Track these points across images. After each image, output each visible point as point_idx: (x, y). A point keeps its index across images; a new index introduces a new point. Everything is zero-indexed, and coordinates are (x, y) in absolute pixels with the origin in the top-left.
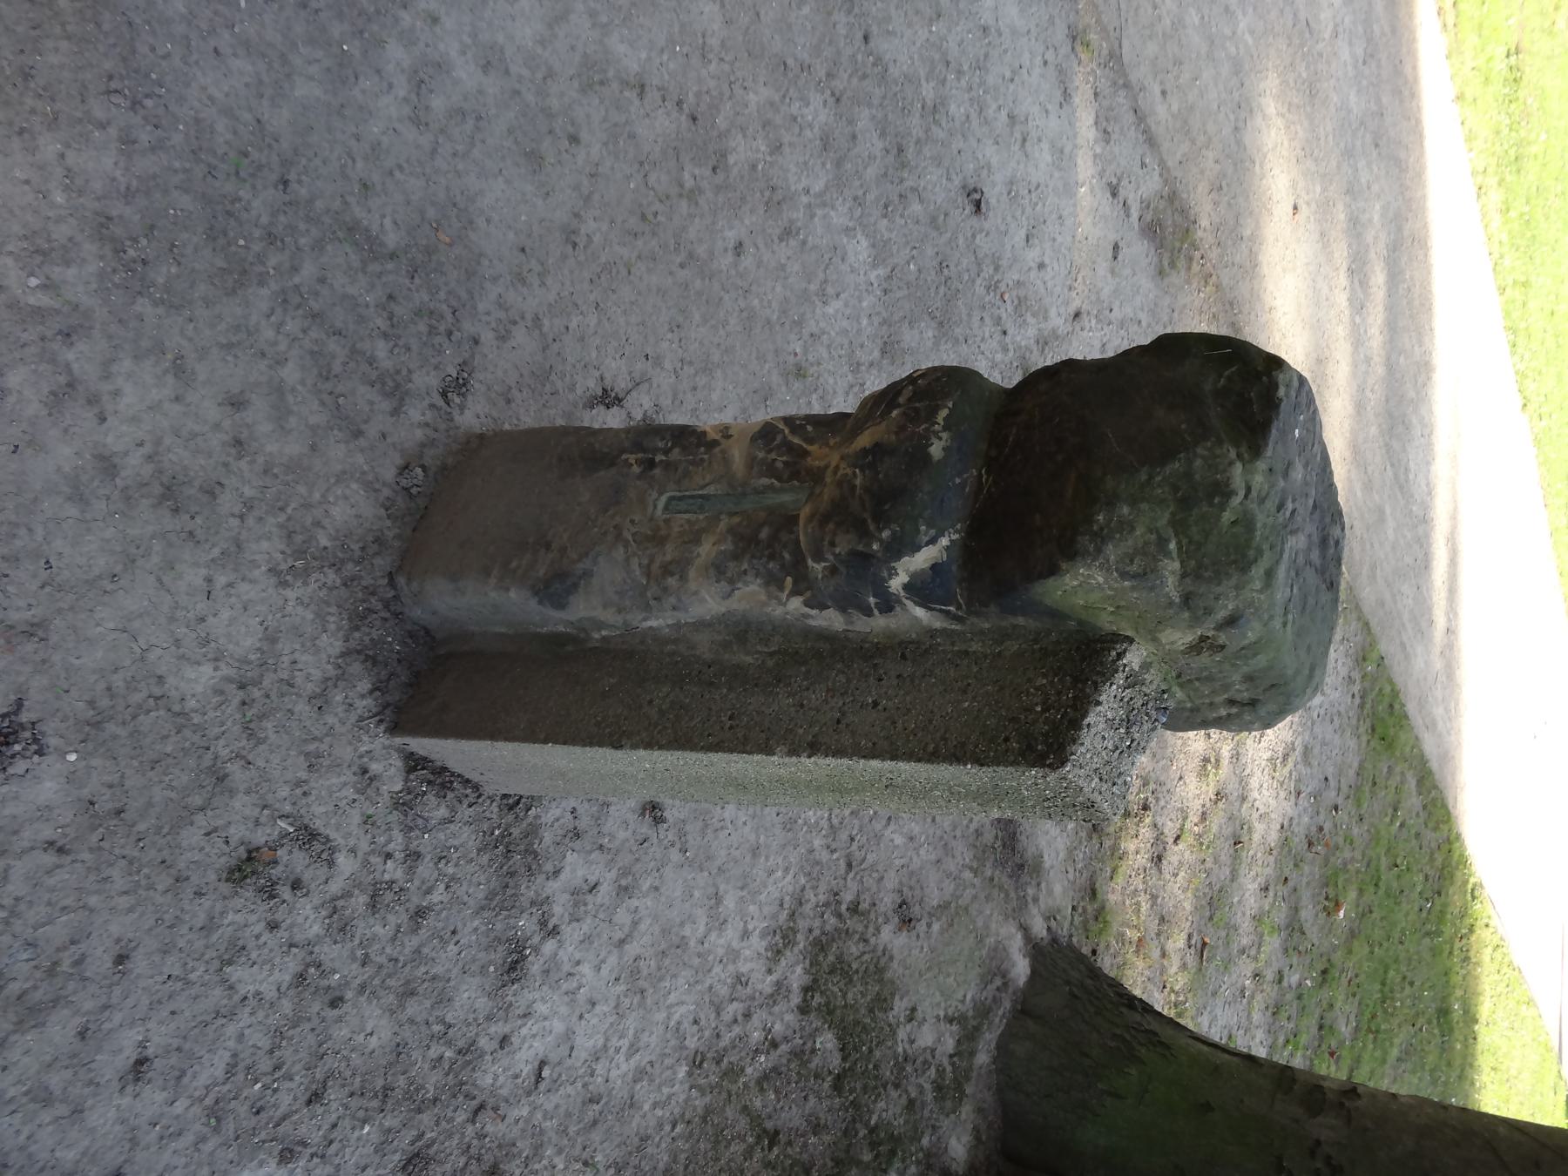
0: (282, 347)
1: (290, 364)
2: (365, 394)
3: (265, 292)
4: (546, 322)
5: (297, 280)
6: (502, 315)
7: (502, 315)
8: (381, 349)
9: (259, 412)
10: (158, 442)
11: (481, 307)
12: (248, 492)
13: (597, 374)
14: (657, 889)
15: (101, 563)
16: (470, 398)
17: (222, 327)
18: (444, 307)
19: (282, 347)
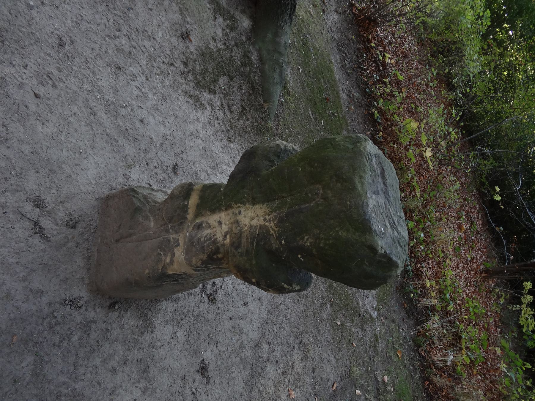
0: (91, 369)
1: (95, 363)
2: (94, 335)
3: (77, 386)
4: (21, 275)
5: (67, 380)
6: (31, 297)
7: (31, 297)
8: (75, 338)
9: (114, 363)
10: (134, 383)
11: (34, 308)
12: (136, 351)
13: (30, 239)
14: (194, 163)
15: (166, 375)
16: (75, 296)
17: (95, 390)
18: (45, 324)
19: (91, 369)
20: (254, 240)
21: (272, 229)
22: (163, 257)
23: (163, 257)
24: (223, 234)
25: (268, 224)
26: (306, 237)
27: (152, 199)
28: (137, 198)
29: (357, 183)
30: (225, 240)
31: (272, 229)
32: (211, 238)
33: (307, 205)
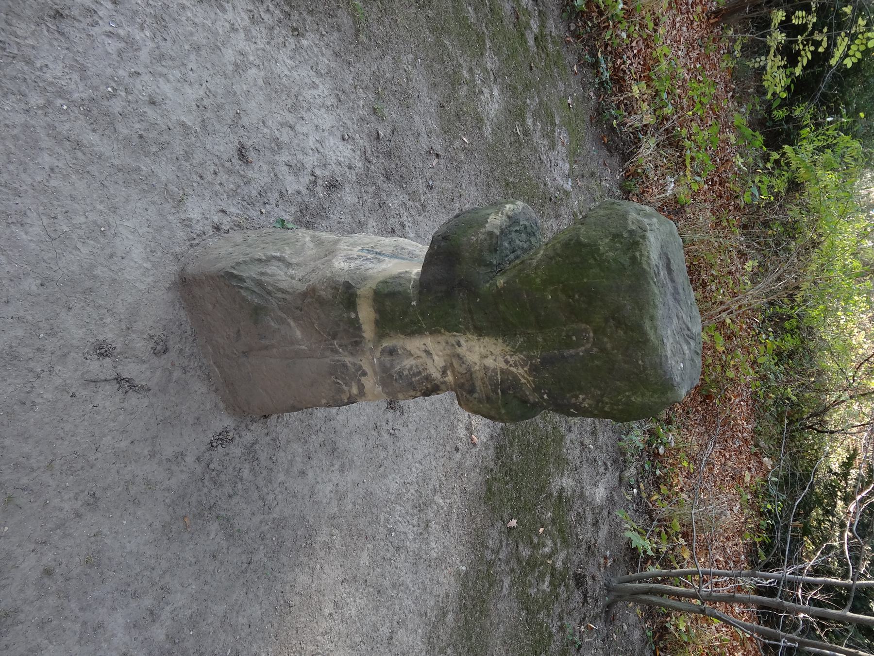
0: (279, 489)
1: (279, 481)
2: (263, 456)
3: (275, 515)
4: (146, 452)
5: (262, 517)
6: (174, 468)
7: (174, 468)
8: (246, 474)
9: (298, 466)
10: (328, 469)
11: (184, 476)
12: (314, 437)
13: (126, 405)
14: (264, 122)
15: (356, 437)
16: (218, 432)
17: (293, 505)
18: (207, 483)
19: (279, 489)
20: (497, 388)
21: (523, 377)
25: (514, 370)
27: (272, 285)
28: (247, 289)
31: (523, 377)
33: (572, 351)
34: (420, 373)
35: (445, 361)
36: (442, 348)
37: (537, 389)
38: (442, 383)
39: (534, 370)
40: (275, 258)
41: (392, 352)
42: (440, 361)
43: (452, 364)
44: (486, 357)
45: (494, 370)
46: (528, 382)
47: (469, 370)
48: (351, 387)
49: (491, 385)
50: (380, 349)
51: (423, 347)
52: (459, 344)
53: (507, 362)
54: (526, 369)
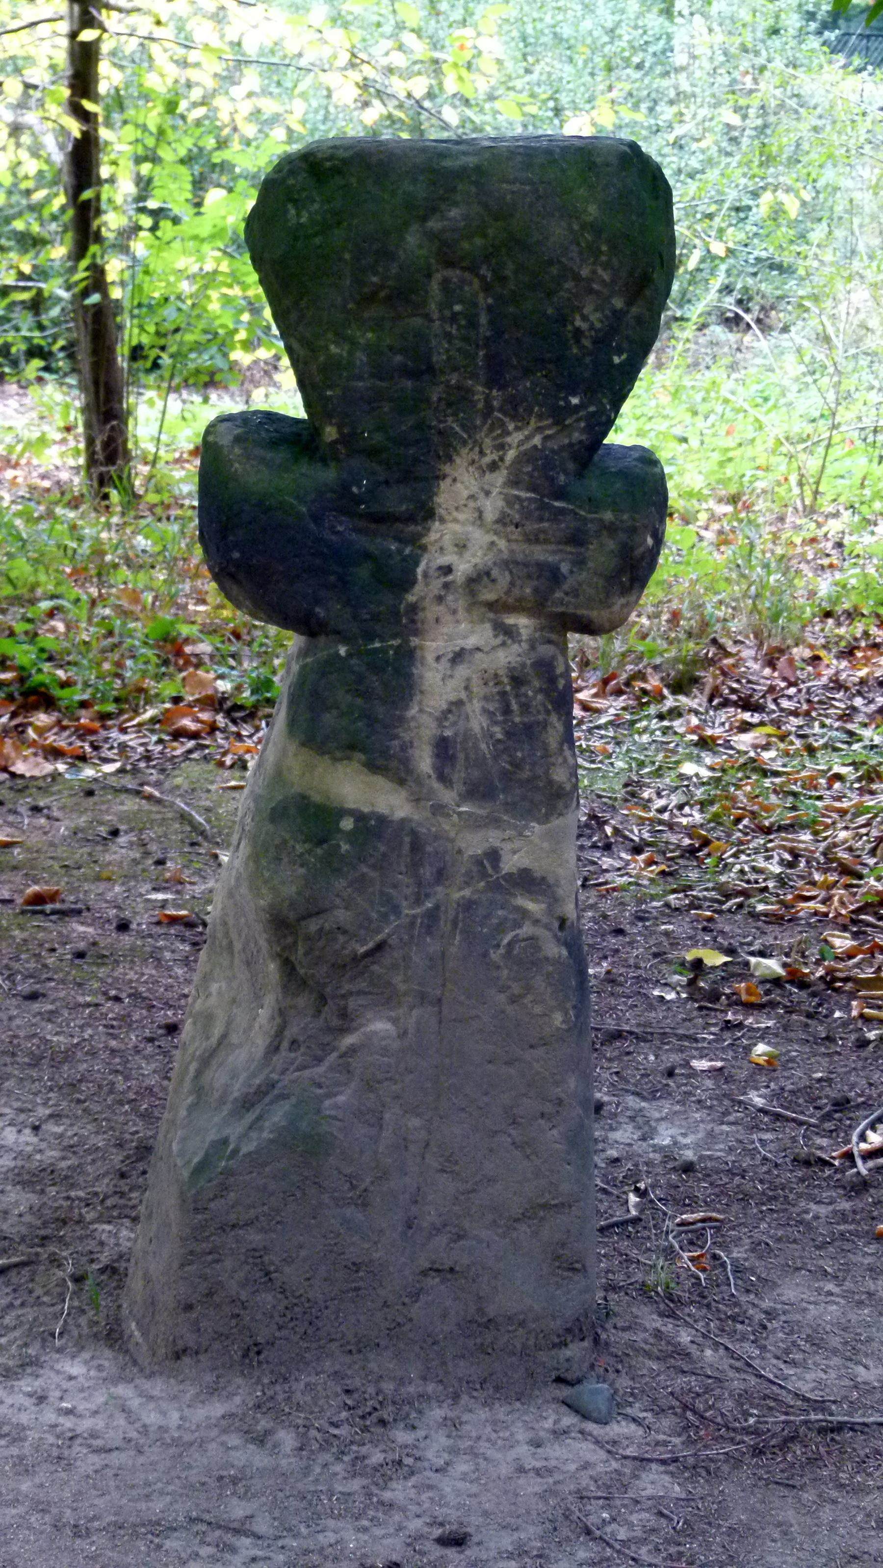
21: (528, 438)
22: (527, 930)
23: (527, 930)
24: (501, 638)
25: (511, 455)
26: (578, 323)
27: (253, 1075)
29: (458, 163)
30: (519, 634)
31: (528, 438)
32: (503, 694)
33: (483, 319)
34: (503, 694)
35: (482, 621)
36: (449, 618)
37: (559, 415)
38: (533, 648)
39: (516, 409)
40: (199, 1074)
41: (444, 750)
42: (477, 635)
43: (491, 606)
44: (480, 513)
45: (510, 501)
46: (539, 429)
47: (507, 564)
48: (524, 913)
49: (541, 519)
50: (436, 785)
51: (444, 663)
52: (447, 570)
53: (494, 467)
54: (511, 427)
